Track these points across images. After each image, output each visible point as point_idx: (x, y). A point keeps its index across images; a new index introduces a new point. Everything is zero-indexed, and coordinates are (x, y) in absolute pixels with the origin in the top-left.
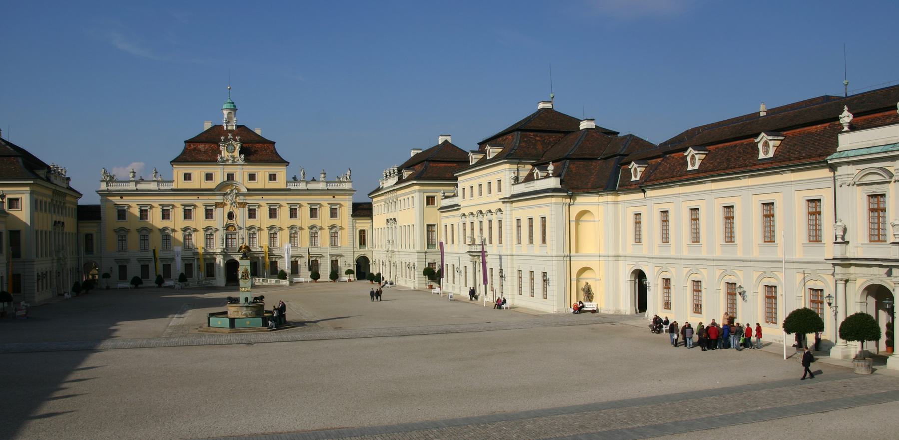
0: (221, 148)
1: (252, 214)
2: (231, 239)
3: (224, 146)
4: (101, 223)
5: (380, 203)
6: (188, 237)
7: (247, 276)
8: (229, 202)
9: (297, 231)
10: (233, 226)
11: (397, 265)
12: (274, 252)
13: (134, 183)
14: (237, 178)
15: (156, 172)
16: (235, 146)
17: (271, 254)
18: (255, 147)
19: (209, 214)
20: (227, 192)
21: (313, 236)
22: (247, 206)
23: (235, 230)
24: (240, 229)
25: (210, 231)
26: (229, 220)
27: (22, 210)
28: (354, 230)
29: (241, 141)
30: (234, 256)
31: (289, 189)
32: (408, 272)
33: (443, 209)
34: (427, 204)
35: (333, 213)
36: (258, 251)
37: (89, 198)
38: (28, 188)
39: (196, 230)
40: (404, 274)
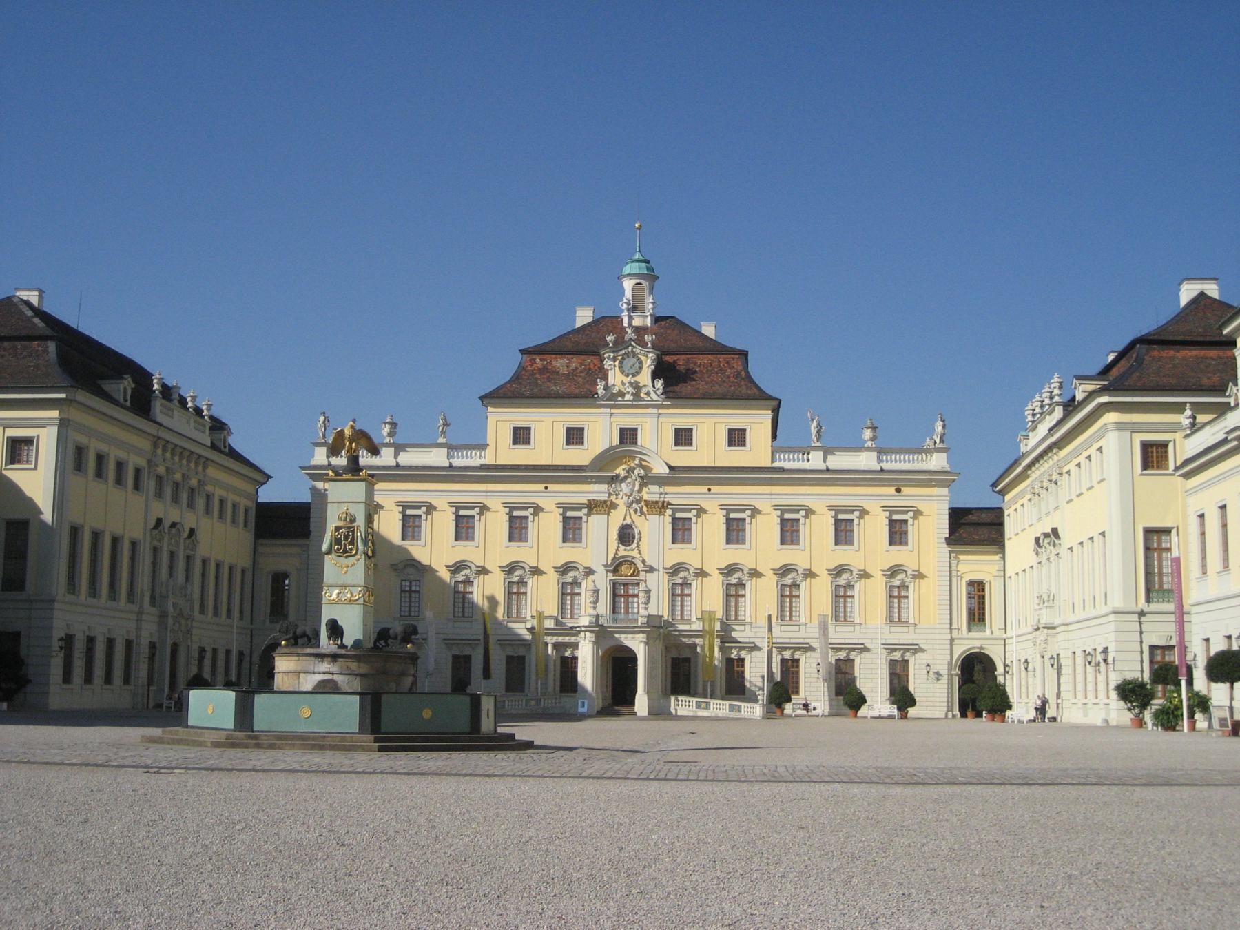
0: (608, 364)
1: (681, 531)
2: (627, 596)
3: (614, 359)
4: (308, 545)
5: (1021, 502)
6: (518, 588)
7: (352, 543)
8: (621, 502)
9: (799, 578)
10: (631, 563)
11: (1063, 661)
12: (734, 634)
13: (392, 450)
14: (646, 439)
15: (446, 425)
16: (643, 358)
17: (726, 637)
18: (695, 364)
19: (571, 529)
20: (618, 476)
21: (842, 595)
22: (669, 512)
23: (636, 573)
24: (651, 569)
25: (571, 574)
26: (622, 547)
27: (36, 468)
28: (954, 579)
29: (655, 346)
30: (623, 636)
31: (781, 470)
32: (1090, 678)
33: (1194, 466)
34: (1146, 465)
35: (897, 533)
36: (694, 627)
38: (55, 413)
39: (537, 571)
40: (1080, 687)
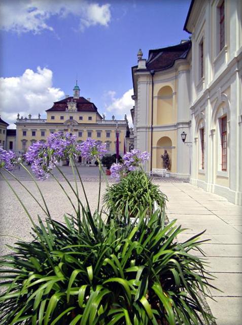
1: (80, 134)
21: (108, 146)
37: (12, 127)
